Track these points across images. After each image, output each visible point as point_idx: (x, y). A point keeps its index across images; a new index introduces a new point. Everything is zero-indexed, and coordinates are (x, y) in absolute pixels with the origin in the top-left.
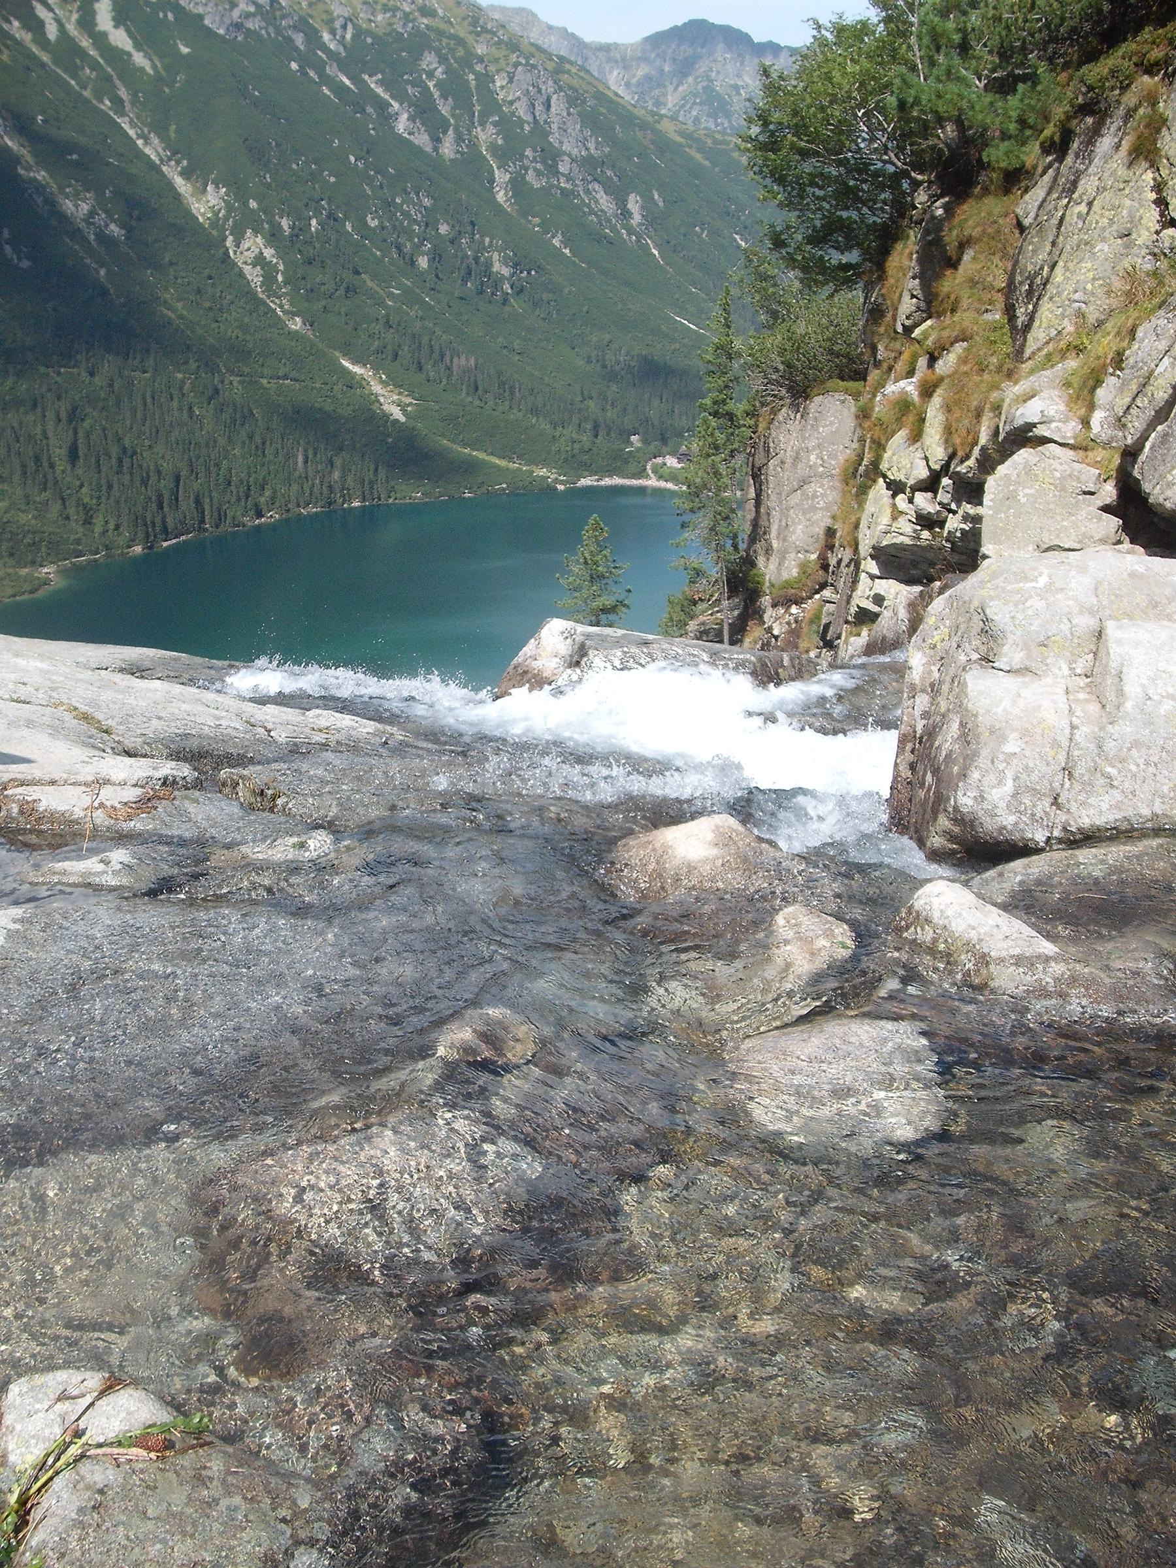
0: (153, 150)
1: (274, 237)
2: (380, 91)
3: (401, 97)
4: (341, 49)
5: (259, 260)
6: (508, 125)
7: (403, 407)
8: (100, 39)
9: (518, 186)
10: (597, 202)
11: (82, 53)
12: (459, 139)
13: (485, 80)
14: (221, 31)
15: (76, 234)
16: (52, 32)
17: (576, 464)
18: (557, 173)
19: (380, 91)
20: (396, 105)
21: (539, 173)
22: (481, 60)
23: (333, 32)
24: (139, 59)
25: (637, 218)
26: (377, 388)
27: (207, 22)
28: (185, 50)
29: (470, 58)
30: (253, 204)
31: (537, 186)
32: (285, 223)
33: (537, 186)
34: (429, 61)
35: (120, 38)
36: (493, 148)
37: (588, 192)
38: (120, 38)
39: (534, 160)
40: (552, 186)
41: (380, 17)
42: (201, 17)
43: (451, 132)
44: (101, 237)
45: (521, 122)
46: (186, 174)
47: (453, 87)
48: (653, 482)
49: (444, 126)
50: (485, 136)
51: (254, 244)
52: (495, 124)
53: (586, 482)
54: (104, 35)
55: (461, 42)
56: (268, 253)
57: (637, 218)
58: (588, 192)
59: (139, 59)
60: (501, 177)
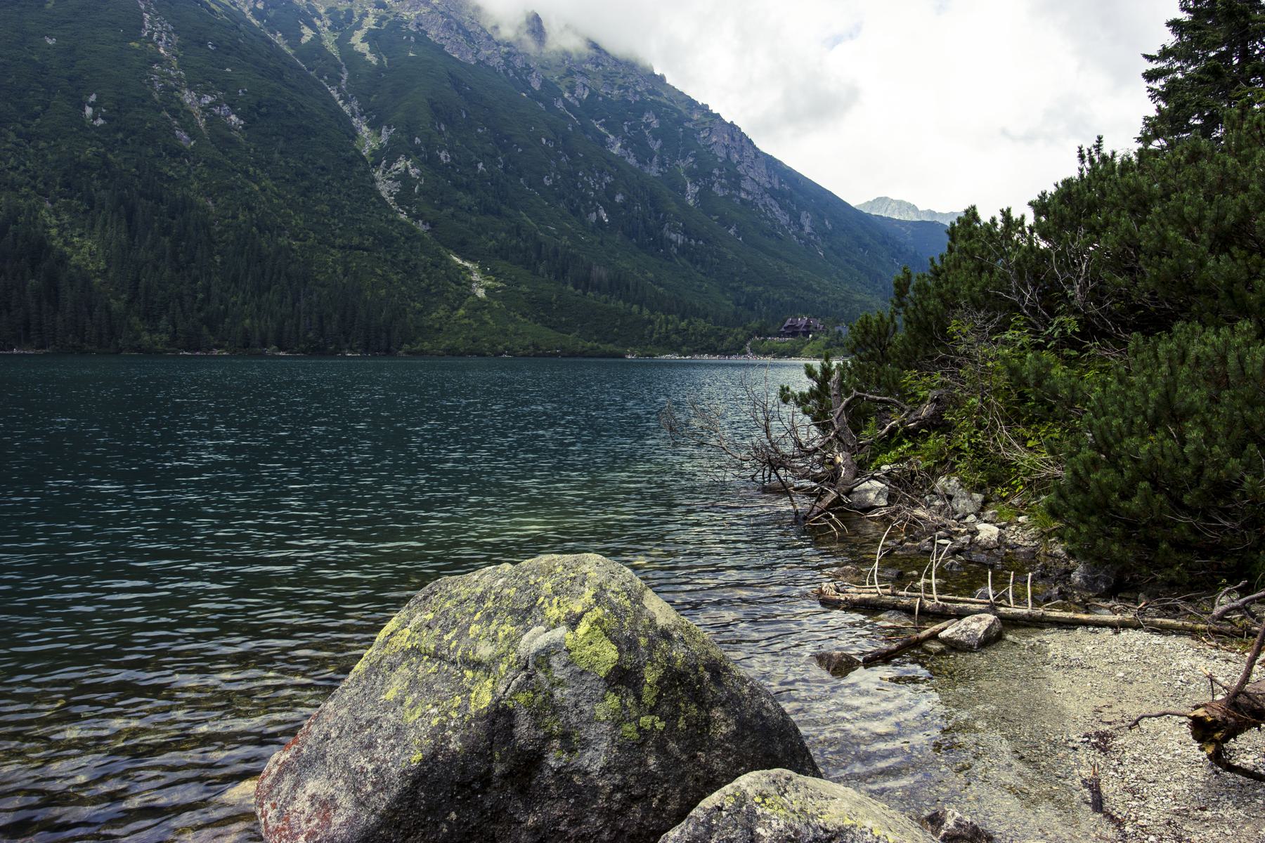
2: (602, 130)
4: (577, 103)
10: (772, 212)
14: (456, 56)
18: (739, 188)
19: (602, 130)
20: (612, 137)
21: (723, 187)
23: (572, 93)
26: (476, 277)
27: (446, 48)
30: (417, 140)
31: (720, 194)
33: (720, 194)
37: (765, 205)
39: (720, 176)
40: (734, 196)
41: (616, 92)
42: (443, 46)
43: (655, 159)
49: (651, 155)
52: (692, 156)
57: (808, 229)
58: (765, 205)
60: (692, 189)
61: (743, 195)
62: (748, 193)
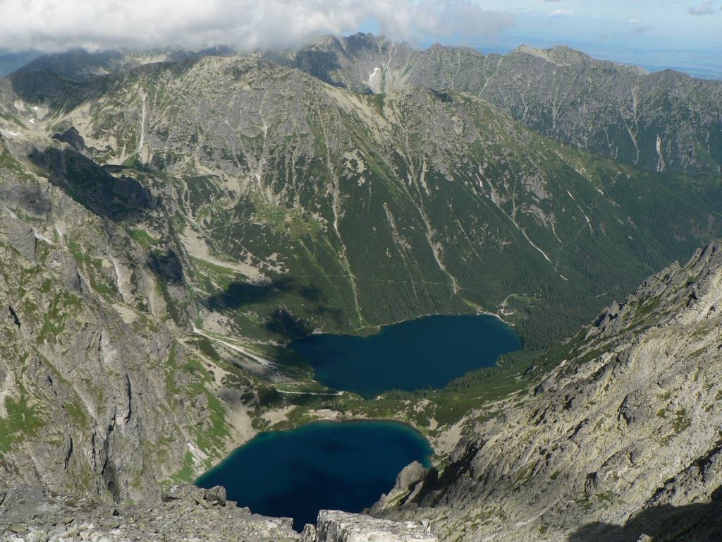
0: (424, 217)
1: (444, 244)
2: (490, 184)
3: (495, 186)
5: (439, 250)
8: (420, 184)
11: (415, 189)
13: (520, 177)
15: (401, 248)
16: (410, 183)
17: (485, 308)
19: (490, 184)
28: (437, 188)
34: (507, 172)
35: (424, 185)
36: (516, 200)
38: (424, 185)
44: (406, 249)
46: (430, 224)
48: (497, 316)
51: (439, 245)
53: (485, 313)
54: (421, 183)
60: (515, 209)
61: (530, 211)
62: (532, 210)
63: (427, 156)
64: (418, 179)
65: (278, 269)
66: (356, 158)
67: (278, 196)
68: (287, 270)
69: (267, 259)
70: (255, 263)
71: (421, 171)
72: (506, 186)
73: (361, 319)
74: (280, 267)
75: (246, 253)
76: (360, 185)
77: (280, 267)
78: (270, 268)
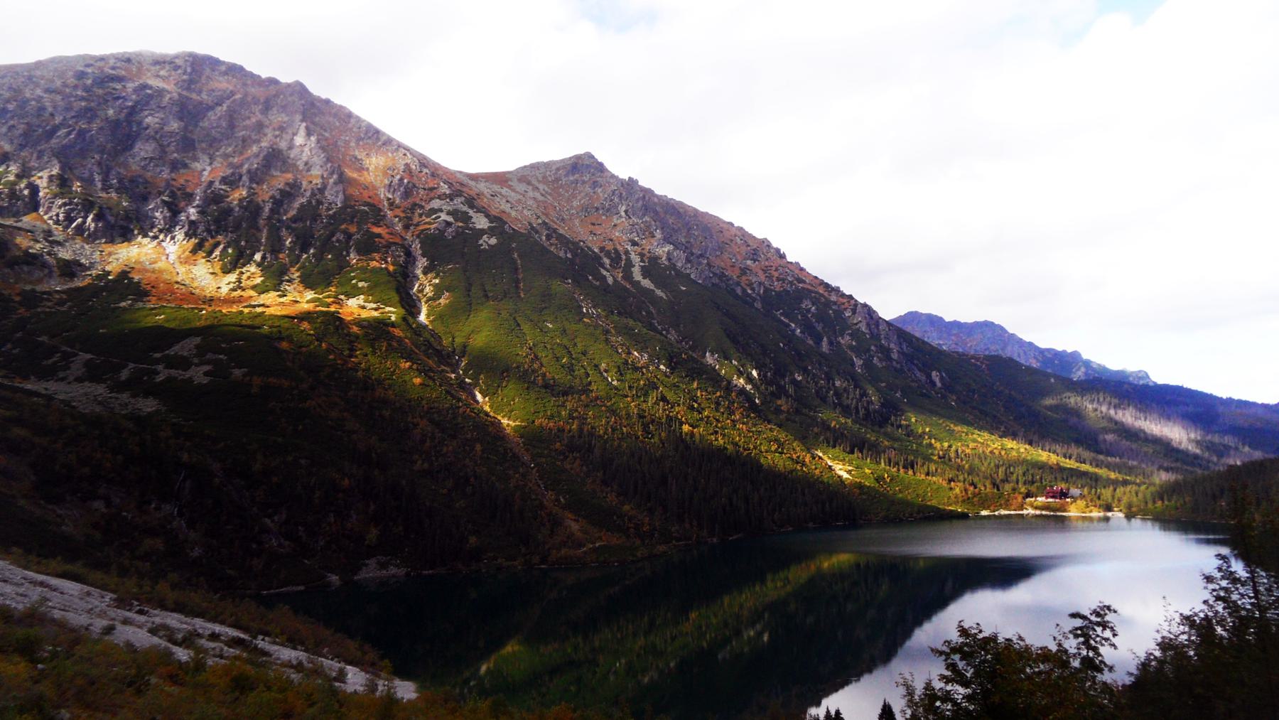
6: (856, 334)
7: (849, 472)
9: (868, 365)
12: (831, 343)
13: (839, 313)
16: (610, 280)
21: (881, 360)
22: (835, 303)
24: (659, 293)
25: (939, 385)
29: (828, 304)
32: (755, 373)
34: (806, 304)
35: (646, 283)
38: (646, 283)
45: (864, 334)
47: (821, 317)
50: (845, 340)
55: (822, 295)
56: (749, 387)
59: (659, 293)
60: (858, 362)
63: (634, 244)
64: (628, 275)
65: (198, 374)
66: (465, 208)
67: (232, 277)
68: (237, 373)
69: (158, 355)
70: (93, 374)
71: (629, 264)
72: (819, 327)
73: (575, 527)
74: (207, 368)
75: (67, 357)
76: (485, 246)
77: (207, 368)
78: (163, 374)
